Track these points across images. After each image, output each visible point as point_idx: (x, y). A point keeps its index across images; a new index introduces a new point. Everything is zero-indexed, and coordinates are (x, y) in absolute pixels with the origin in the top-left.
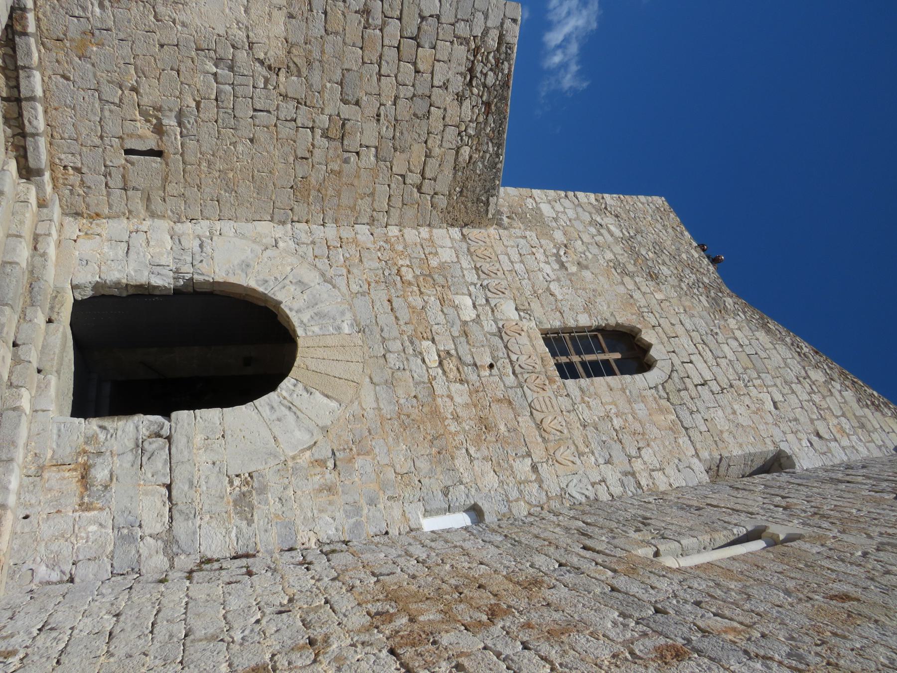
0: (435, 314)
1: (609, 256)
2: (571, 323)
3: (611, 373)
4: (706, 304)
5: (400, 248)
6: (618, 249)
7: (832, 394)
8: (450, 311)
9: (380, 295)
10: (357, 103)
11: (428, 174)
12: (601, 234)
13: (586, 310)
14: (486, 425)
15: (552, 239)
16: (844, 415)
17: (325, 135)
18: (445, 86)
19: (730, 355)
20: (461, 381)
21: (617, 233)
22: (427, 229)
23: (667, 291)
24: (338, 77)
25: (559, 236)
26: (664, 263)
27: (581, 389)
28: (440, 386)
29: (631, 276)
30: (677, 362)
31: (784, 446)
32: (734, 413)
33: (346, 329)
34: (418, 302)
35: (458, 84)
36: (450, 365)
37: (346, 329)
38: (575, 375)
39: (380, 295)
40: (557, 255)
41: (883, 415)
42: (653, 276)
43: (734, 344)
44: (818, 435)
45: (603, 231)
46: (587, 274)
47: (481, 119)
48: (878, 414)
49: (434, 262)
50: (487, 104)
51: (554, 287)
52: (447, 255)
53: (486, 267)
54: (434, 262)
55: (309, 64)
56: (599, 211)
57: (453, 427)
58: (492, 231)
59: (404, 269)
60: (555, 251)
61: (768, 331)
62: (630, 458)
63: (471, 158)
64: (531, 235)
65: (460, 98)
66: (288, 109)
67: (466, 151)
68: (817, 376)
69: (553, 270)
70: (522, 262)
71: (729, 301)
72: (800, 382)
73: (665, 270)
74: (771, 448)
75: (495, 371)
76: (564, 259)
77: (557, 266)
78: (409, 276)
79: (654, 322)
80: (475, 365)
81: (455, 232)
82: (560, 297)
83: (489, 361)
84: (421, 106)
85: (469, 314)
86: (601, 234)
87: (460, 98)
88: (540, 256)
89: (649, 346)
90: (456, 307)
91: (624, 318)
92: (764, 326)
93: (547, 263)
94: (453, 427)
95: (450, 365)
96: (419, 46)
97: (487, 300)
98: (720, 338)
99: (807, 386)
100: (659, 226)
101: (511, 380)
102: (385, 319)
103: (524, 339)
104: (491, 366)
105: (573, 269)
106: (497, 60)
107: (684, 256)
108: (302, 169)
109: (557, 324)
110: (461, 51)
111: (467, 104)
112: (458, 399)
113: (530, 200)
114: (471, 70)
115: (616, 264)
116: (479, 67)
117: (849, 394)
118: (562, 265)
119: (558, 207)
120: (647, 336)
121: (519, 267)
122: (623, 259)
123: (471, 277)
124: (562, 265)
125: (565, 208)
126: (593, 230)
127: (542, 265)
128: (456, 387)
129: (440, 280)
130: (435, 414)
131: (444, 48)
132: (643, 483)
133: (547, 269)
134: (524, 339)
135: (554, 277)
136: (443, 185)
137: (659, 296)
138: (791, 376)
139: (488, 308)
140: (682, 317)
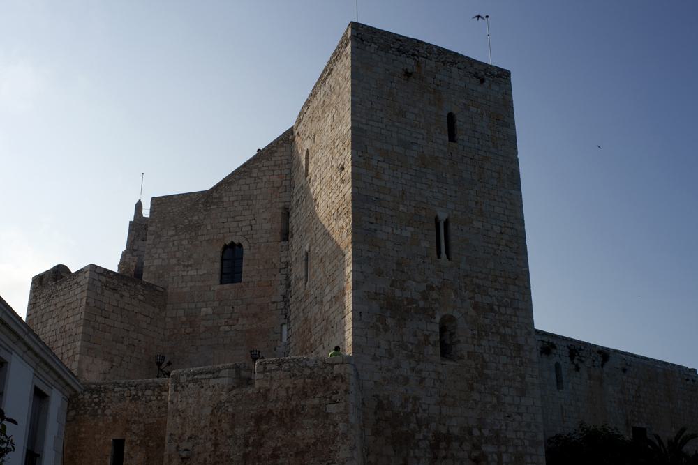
1: (185, 242)
2: (218, 271)
4: (215, 206)
5: (176, 331)
6: (183, 237)
7: (264, 171)
10: (123, 338)
11: (147, 314)
12: (174, 241)
14: (255, 315)
15: (175, 265)
16: (273, 171)
17: (133, 352)
18: (118, 301)
20: (238, 320)
21: (173, 232)
22: (166, 319)
24: (114, 343)
25: (173, 261)
26: (192, 217)
27: (247, 276)
28: (238, 327)
30: (241, 233)
32: (265, 219)
35: (117, 296)
36: (231, 322)
40: (184, 266)
41: (276, 152)
43: (236, 204)
44: (278, 188)
45: (172, 239)
46: (195, 256)
47: (128, 287)
48: (276, 154)
49: (184, 319)
50: (124, 284)
51: (201, 272)
52: (181, 313)
54: (184, 319)
55: (110, 353)
56: (159, 236)
58: (169, 291)
59: (187, 331)
60: (182, 266)
62: (275, 268)
63: (141, 295)
69: (191, 270)
70: (186, 282)
72: (257, 183)
74: (280, 211)
75: (235, 307)
76: (186, 263)
77: (189, 268)
79: (221, 235)
80: (232, 313)
82: (205, 272)
83: (231, 307)
85: (210, 311)
86: (174, 241)
87: (122, 296)
88: (185, 273)
89: (232, 243)
90: (206, 315)
91: (220, 249)
93: (188, 271)
94: (254, 326)
96: (104, 310)
97: (203, 301)
99: (259, 181)
100: (169, 209)
104: (233, 307)
106: (109, 278)
107: (189, 204)
109: (218, 277)
110: (106, 292)
111: (124, 293)
112: (244, 323)
113: (152, 268)
114: (113, 289)
116: (111, 286)
118: (191, 266)
120: (228, 242)
121: (190, 284)
122: (188, 236)
124: (188, 266)
125: (156, 253)
127: (189, 274)
128: (240, 321)
132: (284, 266)
135: (195, 271)
137: (209, 227)
139: (208, 303)
140: (221, 220)
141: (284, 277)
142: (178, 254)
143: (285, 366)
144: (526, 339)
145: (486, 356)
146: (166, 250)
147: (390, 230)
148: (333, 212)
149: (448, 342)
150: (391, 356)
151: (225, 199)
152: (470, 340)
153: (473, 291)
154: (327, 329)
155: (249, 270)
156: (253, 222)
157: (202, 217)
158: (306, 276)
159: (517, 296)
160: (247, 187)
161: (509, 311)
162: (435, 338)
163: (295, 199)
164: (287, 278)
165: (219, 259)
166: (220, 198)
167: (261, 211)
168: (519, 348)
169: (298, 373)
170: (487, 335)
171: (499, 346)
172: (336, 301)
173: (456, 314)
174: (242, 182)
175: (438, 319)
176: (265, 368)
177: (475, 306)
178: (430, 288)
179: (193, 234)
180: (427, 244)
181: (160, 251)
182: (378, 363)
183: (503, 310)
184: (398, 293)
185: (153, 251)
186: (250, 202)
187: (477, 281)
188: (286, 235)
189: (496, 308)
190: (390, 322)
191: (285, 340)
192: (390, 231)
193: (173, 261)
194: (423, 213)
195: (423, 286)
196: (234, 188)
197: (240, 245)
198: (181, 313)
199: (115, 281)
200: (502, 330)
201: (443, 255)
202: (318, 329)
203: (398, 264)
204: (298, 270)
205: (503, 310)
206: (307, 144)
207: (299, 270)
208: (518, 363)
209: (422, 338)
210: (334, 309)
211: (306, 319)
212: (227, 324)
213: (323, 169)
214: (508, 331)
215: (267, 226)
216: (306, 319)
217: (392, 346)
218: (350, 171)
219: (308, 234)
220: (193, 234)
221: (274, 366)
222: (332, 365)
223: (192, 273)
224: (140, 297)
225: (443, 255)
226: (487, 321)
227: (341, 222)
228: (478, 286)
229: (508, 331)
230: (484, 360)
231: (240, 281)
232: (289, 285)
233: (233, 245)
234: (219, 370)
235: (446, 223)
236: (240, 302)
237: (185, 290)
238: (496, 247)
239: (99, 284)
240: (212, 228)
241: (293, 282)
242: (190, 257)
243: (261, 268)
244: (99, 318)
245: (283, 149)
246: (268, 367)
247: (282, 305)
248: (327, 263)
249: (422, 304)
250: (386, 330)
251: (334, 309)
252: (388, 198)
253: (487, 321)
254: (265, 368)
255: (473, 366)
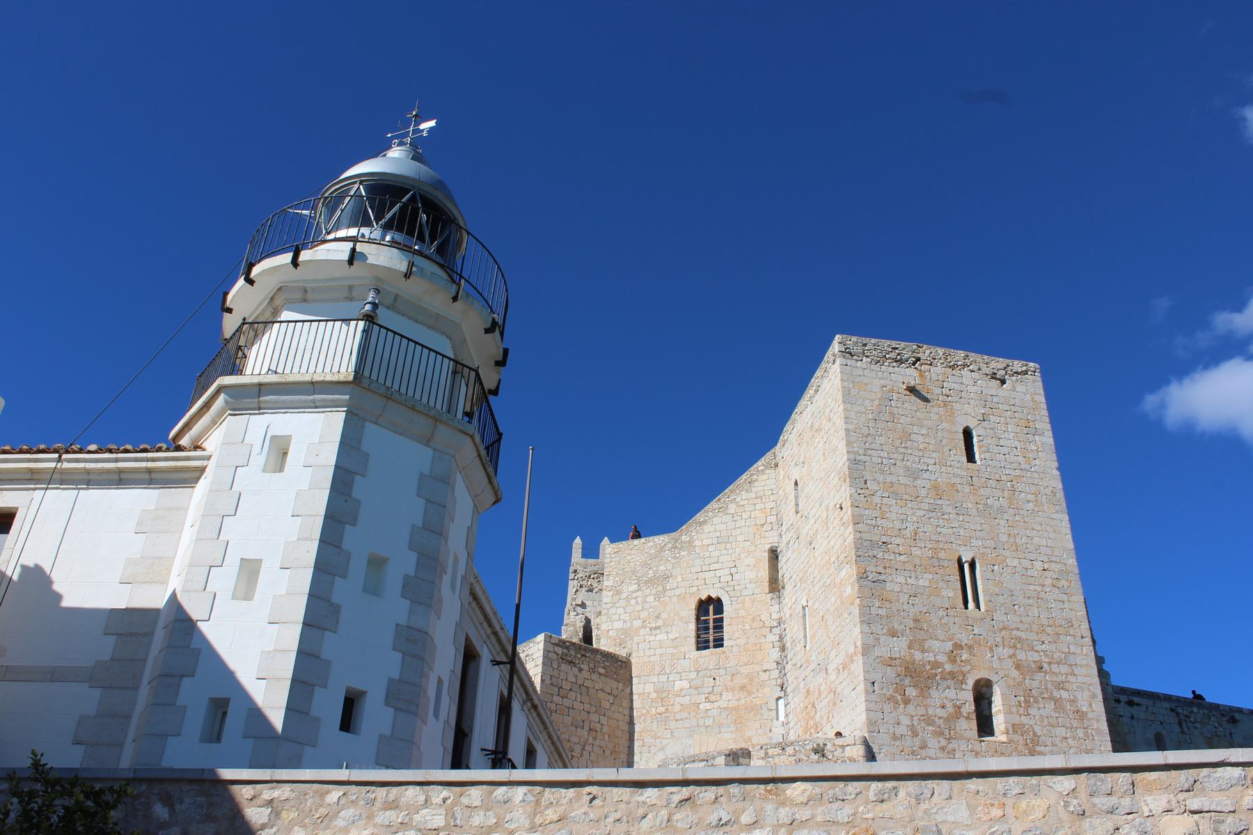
0: (686, 700)
1: (651, 599)
3: (721, 620)
8: (684, 692)
9: (673, 724)
13: (687, 623)
14: (743, 688)
17: (595, 739)
19: (716, 554)
23: (676, 571)
25: (637, 623)
28: (723, 704)
29: (665, 590)
31: (768, 547)
33: (690, 742)
34: (677, 708)
35: (575, 670)
36: (712, 698)
37: (690, 742)
38: (722, 640)
39: (673, 724)
42: (666, 577)
43: (711, 548)
46: (664, 616)
48: (756, 484)
49: (654, 695)
51: (672, 636)
52: (649, 688)
53: (657, 669)
56: (618, 593)
57: (743, 702)
61: (705, 522)
64: (636, 639)
65: (581, 670)
66: (586, 754)
67: (602, 671)
68: (732, 508)
71: (683, 537)
73: (662, 568)
78: (663, 709)
81: (635, 681)
84: (584, 689)
85: (685, 684)
87: (581, 670)
88: (652, 638)
91: (692, 605)
92: (702, 524)
94: (743, 702)
95: (712, 698)
98: (707, 554)
101: (723, 672)
102: (687, 724)
103: (702, 660)
105: (660, 623)
108: (608, 752)
109: (692, 641)
110: (564, 667)
114: (570, 662)
115: (658, 596)
117: (744, 495)
118: (658, 628)
119: (616, 617)
121: (658, 651)
122: (654, 592)
123: (664, 678)
124: (658, 628)
126: (633, 602)
129: (664, 695)
130: (736, 709)
131: (563, 676)
133: (660, 637)
134: (702, 660)
136: (614, 684)
137: (680, 579)
138: (731, 525)
141: (777, 638)
142: (643, 615)
143: (790, 750)
144: (1091, 705)
145: (1037, 729)
146: (628, 610)
147: (903, 581)
148: (833, 559)
149: (986, 713)
150: (915, 734)
151: (697, 543)
152: (1014, 710)
153: (1015, 647)
154: (834, 704)
155: (730, 631)
156: (733, 570)
157: (670, 567)
158: (805, 637)
159: (1073, 649)
160: (723, 527)
161: (1064, 669)
162: (970, 707)
163: (785, 539)
164: (781, 638)
165: (693, 618)
166: (690, 542)
167: (743, 556)
168: (1081, 715)
169: (802, 756)
170: (1036, 701)
171: (1053, 714)
172: (844, 669)
173: (993, 678)
174: (716, 520)
175: (970, 683)
176: (766, 754)
177: (1018, 667)
178: (958, 646)
179: (660, 588)
180: (952, 592)
181: (620, 611)
182: (898, 743)
183: (1055, 668)
184: (918, 656)
185: (612, 611)
186: (729, 546)
187: (1018, 634)
188: (775, 585)
189: (1045, 666)
190: (911, 692)
191: (782, 717)
192: (903, 581)
193: (637, 623)
194: (942, 555)
195: (949, 646)
196: (707, 528)
197: (719, 601)
198: (649, 688)
199: (572, 652)
200: (1056, 694)
201: (971, 604)
202: (825, 702)
203: (916, 620)
204: (793, 630)
205: (1055, 668)
206: (795, 474)
207: (795, 629)
208: (1081, 735)
209: (950, 709)
210: (840, 679)
211: (808, 691)
212: (708, 700)
213: (817, 505)
214: (1065, 695)
215: (751, 575)
216: (808, 691)
217: (915, 723)
218: (850, 513)
219: (804, 585)
220: (660, 588)
221: (778, 751)
222: (843, 747)
223: (660, 637)
224: (602, 671)
225: (971, 604)
226: (1035, 684)
227: (843, 573)
228: (1019, 640)
229: (1065, 695)
230: (1034, 734)
231: (722, 646)
232: (783, 649)
233: (710, 599)
234: (714, 758)
235: (972, 565)
236: (723, 672)
237: (652, 659)
238: (1039, 588)
239: (555, 657)
240: (683, 580)
241: (788, 645)
242: (658, 617)
243: (747, 627)
244: (556, 699)
245: (765, 477)
246: (770, 752)
247: (776, 673)
248: (830, 622)
249: (948, 667)
250: (907, 702)
251: (840, 679)
252: (898, 541)
253: (1035, 684)
254: (766, 754)
255: (1022, 742)
